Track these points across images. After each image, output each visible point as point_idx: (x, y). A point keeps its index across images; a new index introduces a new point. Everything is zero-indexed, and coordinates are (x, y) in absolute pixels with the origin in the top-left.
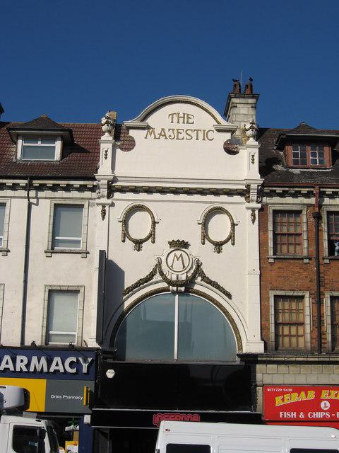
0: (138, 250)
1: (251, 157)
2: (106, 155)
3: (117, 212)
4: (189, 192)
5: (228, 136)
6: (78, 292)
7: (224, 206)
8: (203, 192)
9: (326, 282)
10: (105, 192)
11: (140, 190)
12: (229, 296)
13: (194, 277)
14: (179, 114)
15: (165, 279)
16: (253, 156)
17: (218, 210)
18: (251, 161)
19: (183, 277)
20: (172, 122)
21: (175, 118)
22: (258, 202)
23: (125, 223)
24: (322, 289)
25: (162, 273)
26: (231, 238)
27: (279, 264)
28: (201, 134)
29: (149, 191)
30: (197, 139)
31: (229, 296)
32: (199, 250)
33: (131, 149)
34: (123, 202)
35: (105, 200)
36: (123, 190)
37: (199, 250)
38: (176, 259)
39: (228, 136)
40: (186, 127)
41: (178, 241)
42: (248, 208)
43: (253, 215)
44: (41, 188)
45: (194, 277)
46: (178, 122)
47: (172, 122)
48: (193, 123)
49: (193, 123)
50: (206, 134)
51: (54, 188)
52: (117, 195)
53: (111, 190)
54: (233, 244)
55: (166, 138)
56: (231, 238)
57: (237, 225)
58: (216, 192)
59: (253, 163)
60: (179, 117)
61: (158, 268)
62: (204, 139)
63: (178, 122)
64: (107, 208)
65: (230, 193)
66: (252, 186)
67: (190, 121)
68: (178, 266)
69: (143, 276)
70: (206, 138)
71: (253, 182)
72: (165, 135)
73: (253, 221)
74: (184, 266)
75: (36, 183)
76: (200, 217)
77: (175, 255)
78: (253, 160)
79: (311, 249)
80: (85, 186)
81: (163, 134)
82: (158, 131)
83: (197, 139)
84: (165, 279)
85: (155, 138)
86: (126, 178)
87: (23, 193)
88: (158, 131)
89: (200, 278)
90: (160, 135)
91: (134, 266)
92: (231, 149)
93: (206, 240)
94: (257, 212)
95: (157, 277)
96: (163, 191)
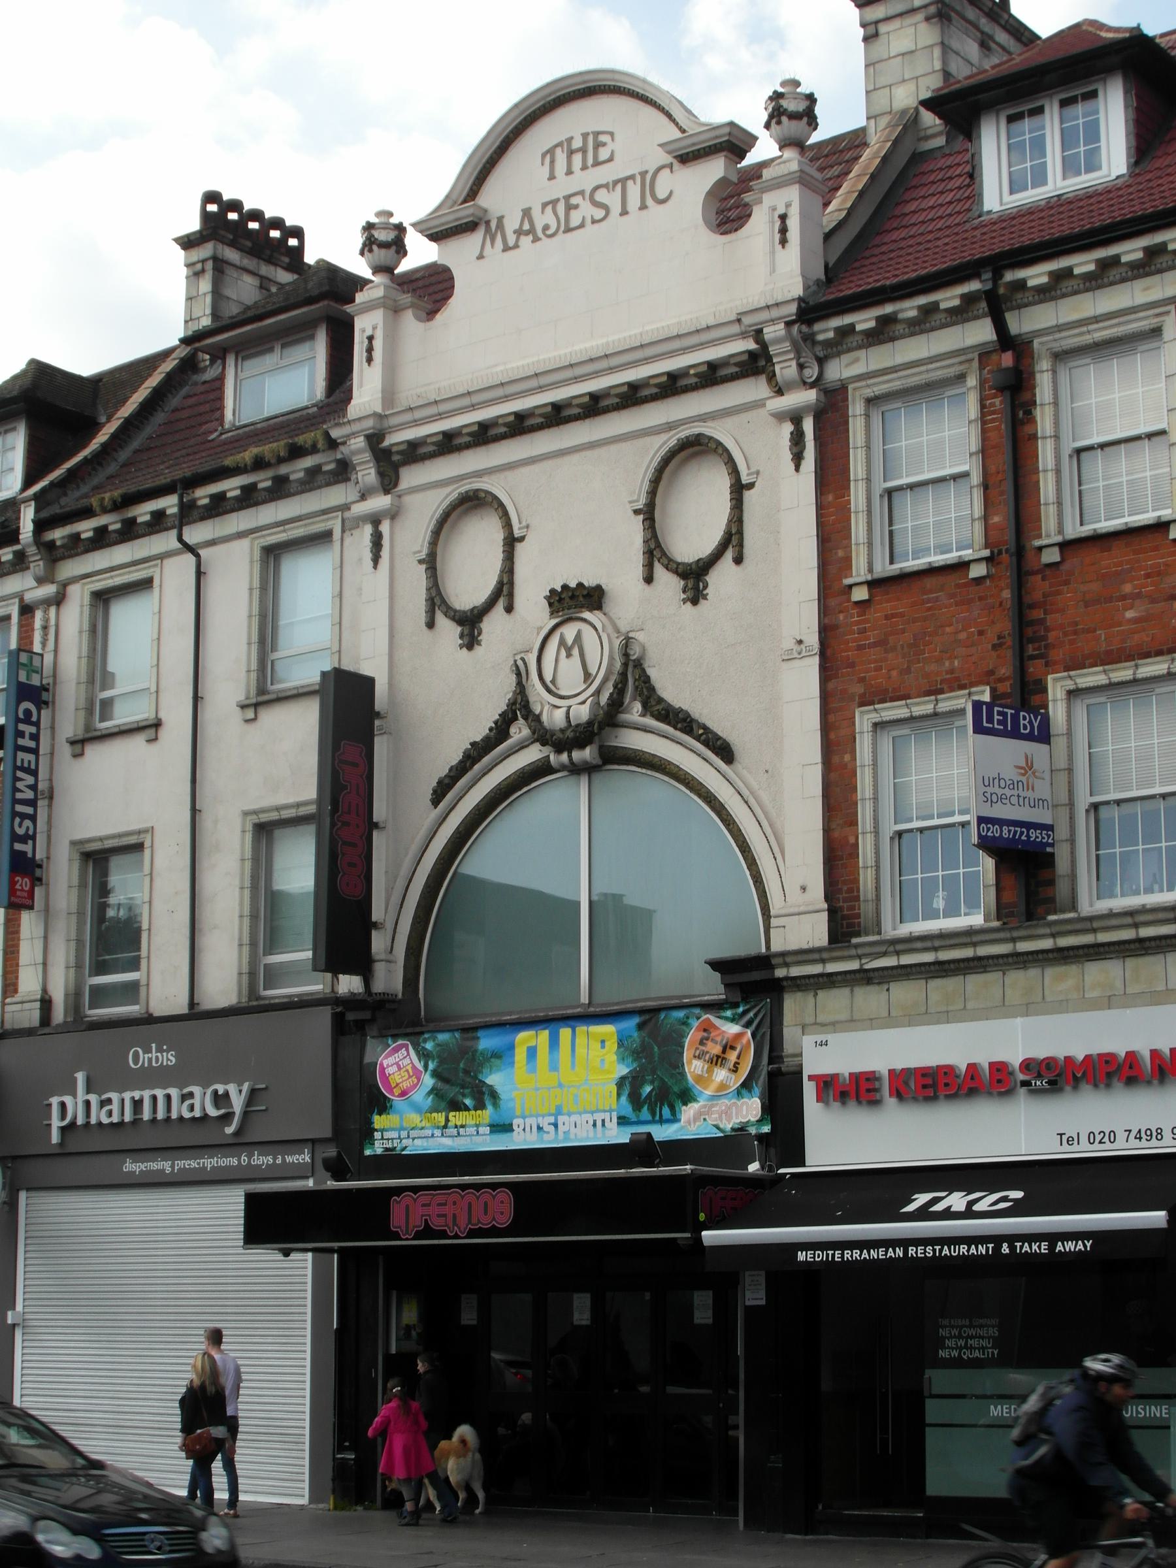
0: (695, 601)
1: (778, 224)
2: (370, 350)
3: (410, 536)
4: (595, 406)
5: (715, 169)
6: (139, 847)
7: (711, 430)
8: (632, 396)
9: (1052, 636)
10: (368, 474)
11: (646, 392)
12: (724, 751)
13: (616, 704)
14: (570, 140)
15: (542, 736)
16: (783, 218)
17: (695, 447)
18: (777, 236)
19: (582, 713)
20: (552, 177)
21: (561, 157)
22: (807, 385)
23: (431, 563)
24: (1033, 668)
25: (533, 719)
26: (733, 541)
27: (886, 605)
28: (634, 190)
29: (484, 435)
30: (624, 212)
31: (724, 751)
32: (642, 606)
33: (750, 215)
34: (429, 487)
35: (380, 502)
36: (414, 453)
37: (642, 606)
38: (563, 653)
39: (715, 169)
40: (586, 180)
41: (565, 587)
42: (780, 416)
43: (797, 439)
44: (219, 507)
45: (616, 704)
46: (569, 172)
47: (552, 177)
48: (610, 159)
49: (610, 159)
50: (648, 181)
51: (249, 498)
52: (411, 477)
53: (391, 462)
54: (738, 560)
55: (536, 239)
56: (733, 541)
57: (751, 486)
58: (673, 386)
59: (784, 242)
60: (571, 152)
61: (519, 707)
62: (643, 207)
63: (569, 172)
64: (385, 527)
65: (712, 376)
66: (770, 333)
67: (604, 154)
68: (569, 676)
69: (480, 730)
70: (649, 201)
71: (764, 316)
72: (532, 231)
73: (798, 458)
74: (587, 676)
75: (203, 495)
76: (632, 485)
77: (562, 642)
78: (784, 230)
79: (996, 519)
80: (932, 309)
81: (528, 230)
82: (512, 223)
83: (624, 212)
84: (542, 736)
85: (506, 248)
86: (438, 407)
87: (167, 541)
88: (512, 223)
89: (638, 706)
90: (519, 233)
91: (446, 698)
92: (729, 210)
93: (659, 570)
94: (808, 426)
95: (520, 731)
96: (519, 426)
